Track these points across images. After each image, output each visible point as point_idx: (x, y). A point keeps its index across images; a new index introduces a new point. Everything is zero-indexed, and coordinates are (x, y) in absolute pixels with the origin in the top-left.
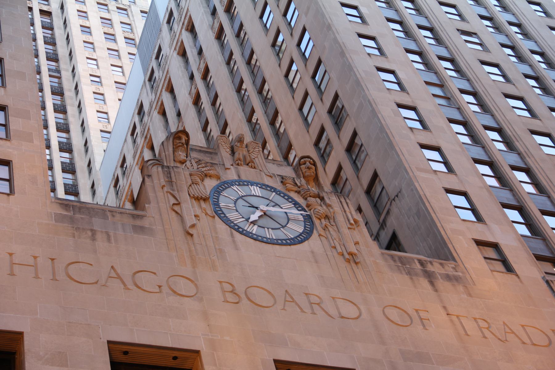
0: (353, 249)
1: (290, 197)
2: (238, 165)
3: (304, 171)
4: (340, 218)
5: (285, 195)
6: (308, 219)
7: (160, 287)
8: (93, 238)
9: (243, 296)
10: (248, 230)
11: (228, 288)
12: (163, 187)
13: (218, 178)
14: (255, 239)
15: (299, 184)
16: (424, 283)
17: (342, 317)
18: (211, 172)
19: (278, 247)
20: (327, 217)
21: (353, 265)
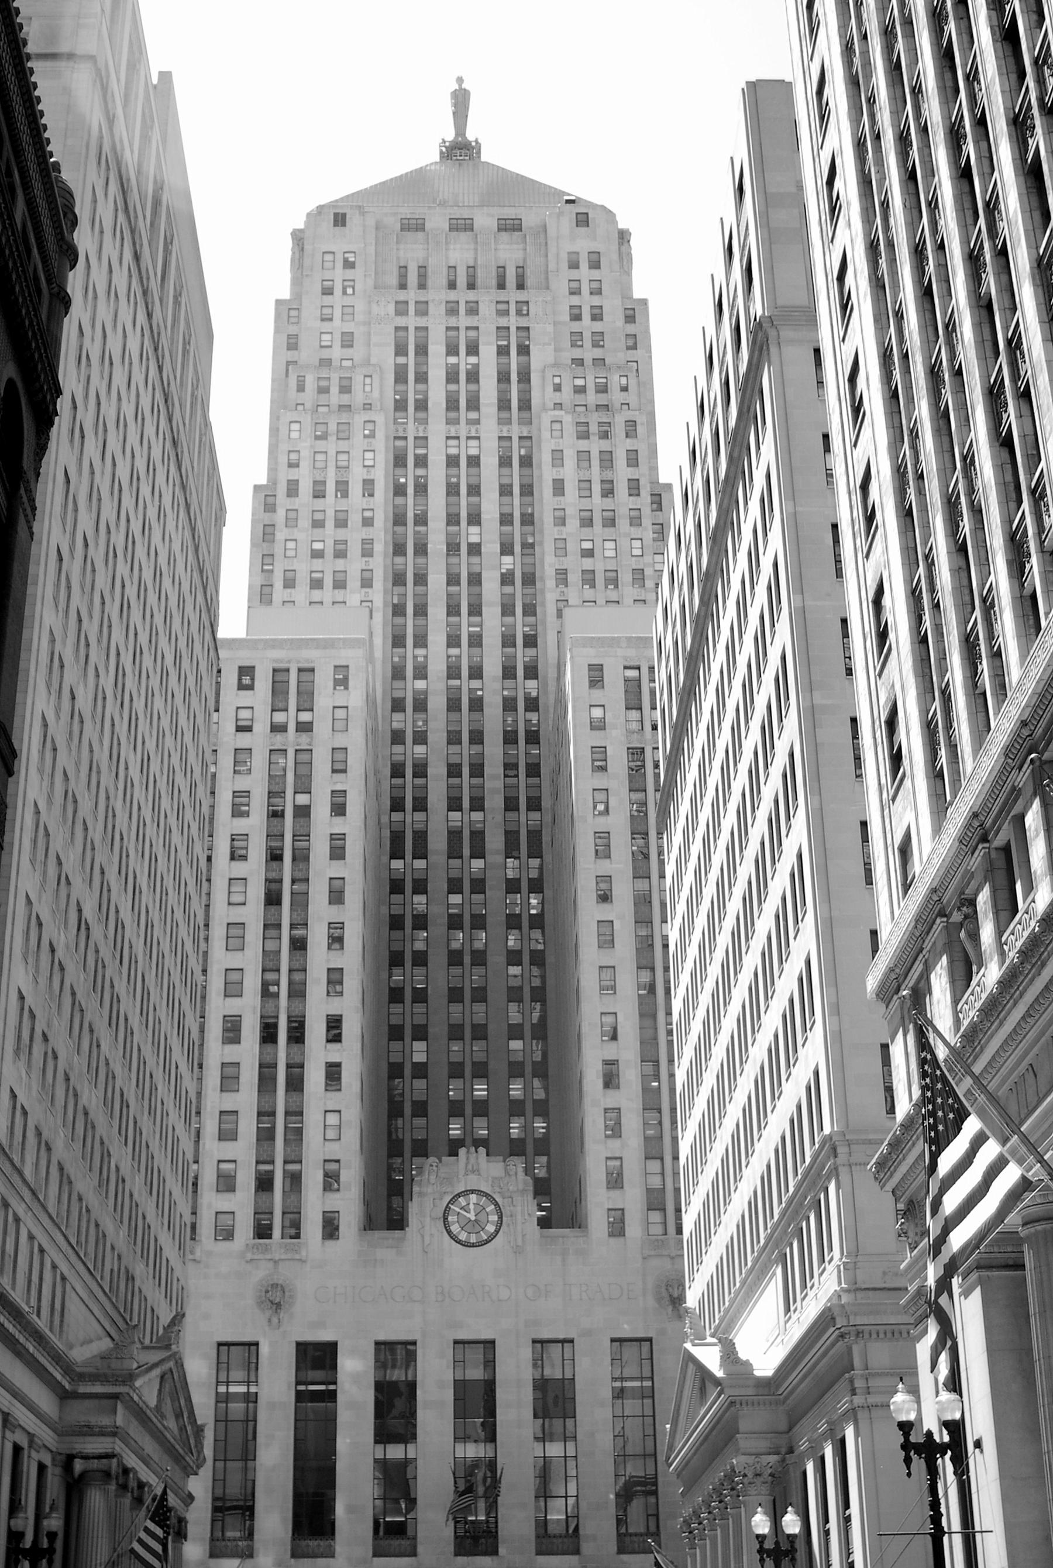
0: (520, 1243)
4: (519, 1217)
6: (501, 1217)
17: (499, 1300)
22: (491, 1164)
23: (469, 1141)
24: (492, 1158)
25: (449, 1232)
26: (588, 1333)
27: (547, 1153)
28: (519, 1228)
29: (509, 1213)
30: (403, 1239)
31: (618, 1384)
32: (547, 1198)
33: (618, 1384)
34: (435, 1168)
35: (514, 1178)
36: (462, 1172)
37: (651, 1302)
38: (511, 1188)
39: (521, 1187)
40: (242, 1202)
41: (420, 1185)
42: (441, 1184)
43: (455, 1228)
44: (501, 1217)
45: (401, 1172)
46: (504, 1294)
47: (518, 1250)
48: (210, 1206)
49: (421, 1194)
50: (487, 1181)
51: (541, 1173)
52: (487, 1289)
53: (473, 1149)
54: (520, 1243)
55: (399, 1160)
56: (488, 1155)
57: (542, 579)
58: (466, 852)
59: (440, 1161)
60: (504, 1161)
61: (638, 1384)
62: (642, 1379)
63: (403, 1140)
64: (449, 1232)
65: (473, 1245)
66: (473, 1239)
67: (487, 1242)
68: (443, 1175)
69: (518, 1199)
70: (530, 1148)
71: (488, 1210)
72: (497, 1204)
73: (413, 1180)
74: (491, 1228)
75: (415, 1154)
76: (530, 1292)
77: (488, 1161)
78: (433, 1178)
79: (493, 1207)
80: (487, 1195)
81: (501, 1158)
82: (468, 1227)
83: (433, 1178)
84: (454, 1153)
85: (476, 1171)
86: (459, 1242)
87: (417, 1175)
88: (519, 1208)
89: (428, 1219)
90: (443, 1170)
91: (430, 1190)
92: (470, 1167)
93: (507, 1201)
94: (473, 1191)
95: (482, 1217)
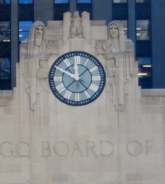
0: (122, 102)
1: (97, 61)
2: (72, 38)
3: (111, 34)
4: (121, 77)
5: (95, 59)
6: (104, 78)
7: (12, 152)
9: (52, 150)
10: (65, 98)
11: (46, 145)
12: (23, 74)
13: (57, 54)
14: (69, 104)
15: (105, 48)
18: (54, 52)
19: (79, 107)
20: (114, 76)
21: (120, 112)
22: (94, 28)
23: (73, 5)
24: (96, 22)
25: (55, 92)
27: (148, 17)
28: (122, 87)
29: (111, 74)
30: (11, 98)
32: (149, 60)
34: (40, 31)
35: (116, 40)
36: (66, 35)
38: (114, 50)
39: (123, 48)
41: (27, 48)
42: (47, 46)
43: (60, 88)
44: (104, 78)
45: (9, 35)
46: (107, 149)
47: (120, 109)
49: (27, 56)
50: (91, 43)
51: (143, 36)
52: (90, 145)
53: (77, 13)
54: (122, 102)
55: (6, 24)
56: (91, 18)
59: (46, 25)
60: (107, 24)
63: (10, 5)
64: (55, 92)
65: (77, 104)
66: (78, 98)
67: (91, 101)
68: (48, 38)
69: (120, 60)
70: (132, 12)
71: (91, 70)
72: (100, 65)
73: (19, 43)
74: (94, 88)
75: (22, 18)
76: (132, 148)
77: (92, 25)
78: (39, 40)
79: (96, 68)
80: (90, 56)
81: (104, 22)
82: (73, 87)
83: (39, 40)
84: (59, 17)
85: (80, 34)
86: (64, 101)
87: (24, 38)
88: (121, 69)
89: (34, 80)
90: (49, 33)
91: (36, 52)
92: (74, 30)
93: (110, 62)
94: (77, 53)
95: (86, 77)
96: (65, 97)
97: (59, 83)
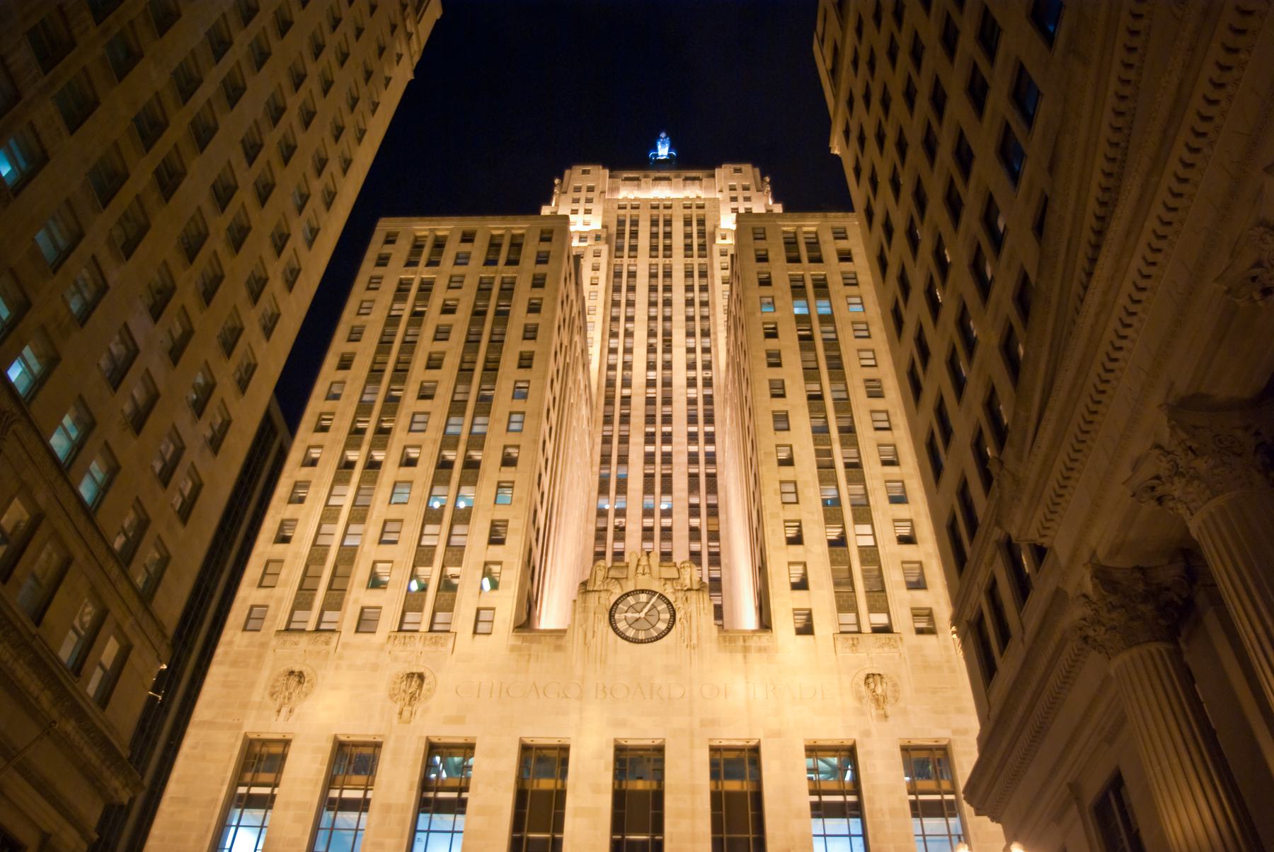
8: (529, 661)
16: (739, 656)
26: (778, 734)
31: (815, 798)
33: (815, 798)
37: (850, 701)
40: (389, 602)
43: (622, 626)
44: (673, 616)
48: (356, 601)
57: (715, 333)
58: (658, 489)
61: (840, 798)
62: (842, 793)
64: (615, 630)
65: (642, 642)
66: (642, 636)
67: (657, 638)
72: (669, 603)
74: (662, 626)
82: (637, 625)
92: (640, 570)
94: (643, 591)
96: (628, 634)
97: (620, 620)
